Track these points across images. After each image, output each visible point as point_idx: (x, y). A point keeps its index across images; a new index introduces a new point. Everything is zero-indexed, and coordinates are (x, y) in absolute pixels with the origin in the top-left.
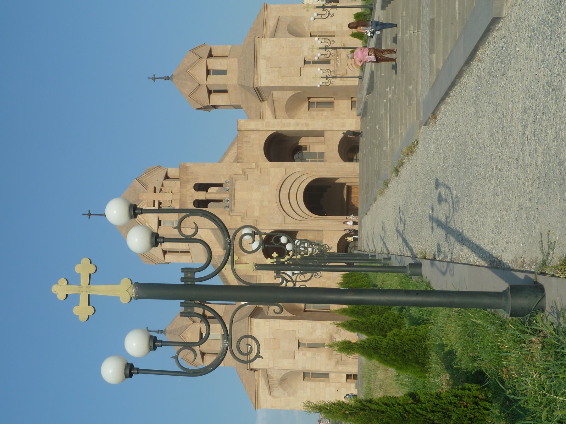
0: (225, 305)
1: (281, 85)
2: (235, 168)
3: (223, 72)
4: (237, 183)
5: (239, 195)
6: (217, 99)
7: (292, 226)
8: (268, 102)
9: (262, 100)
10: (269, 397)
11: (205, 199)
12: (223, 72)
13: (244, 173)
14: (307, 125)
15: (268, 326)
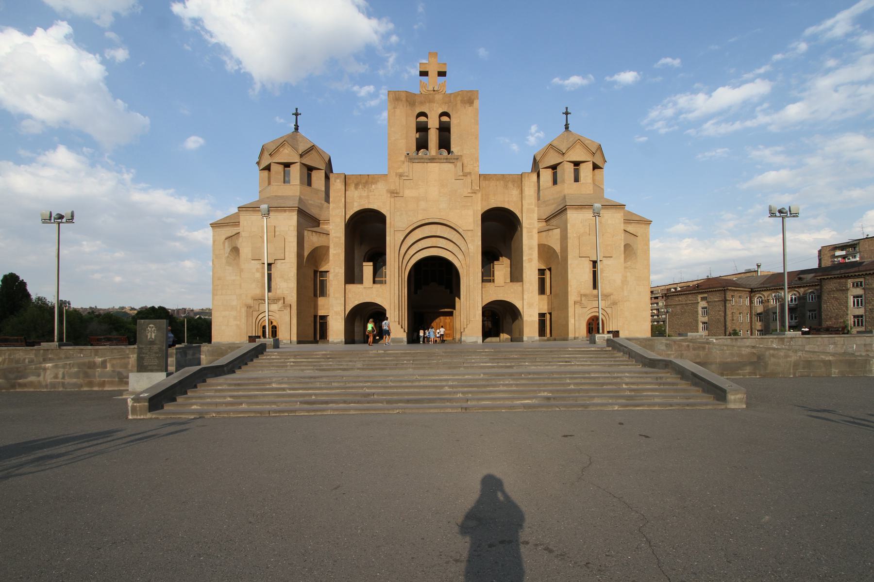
0: (323, 189)
1: (569, 235)
2: (472, 164)
3: (577, 179)
4: (450, 166)
5: (434, 167)
6: (546, 176)
7: (390, 240)
8: (544, 226)
9: (547, 220)
10: (224, 237)
11: (429, 127)
12: (577, 179)
13: (465, 175)
14: (530, 260)
15: (289, 229)
